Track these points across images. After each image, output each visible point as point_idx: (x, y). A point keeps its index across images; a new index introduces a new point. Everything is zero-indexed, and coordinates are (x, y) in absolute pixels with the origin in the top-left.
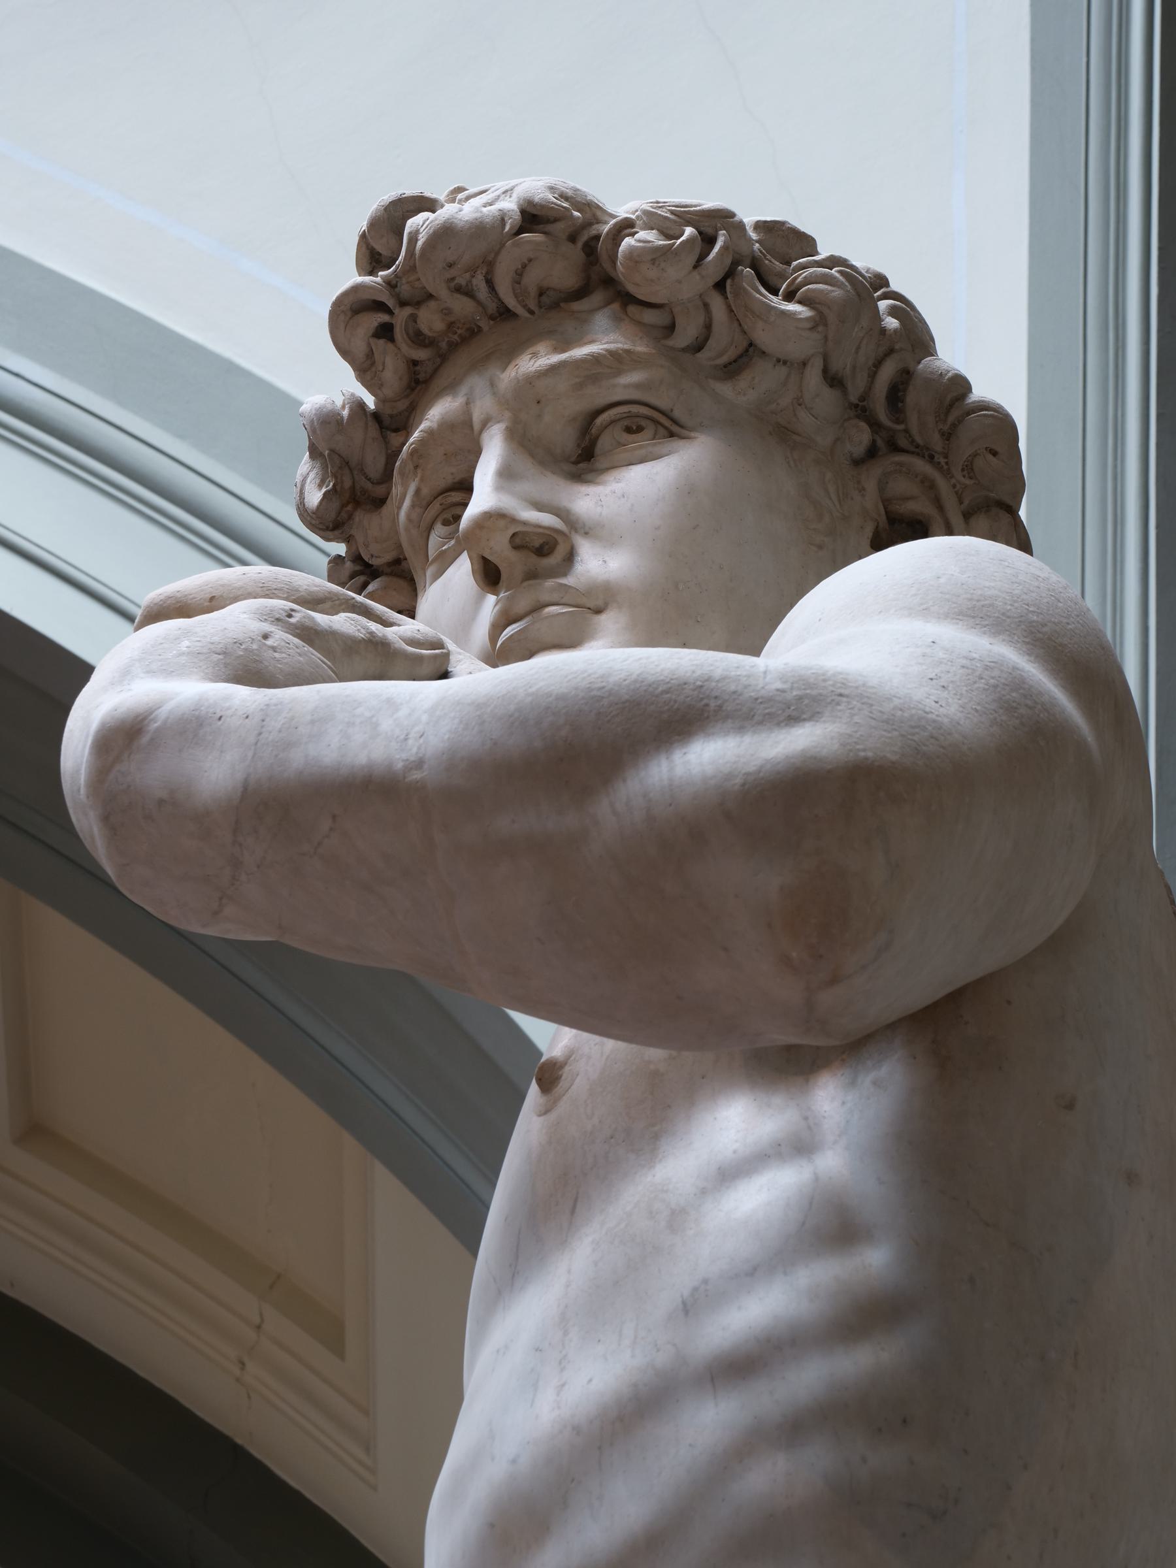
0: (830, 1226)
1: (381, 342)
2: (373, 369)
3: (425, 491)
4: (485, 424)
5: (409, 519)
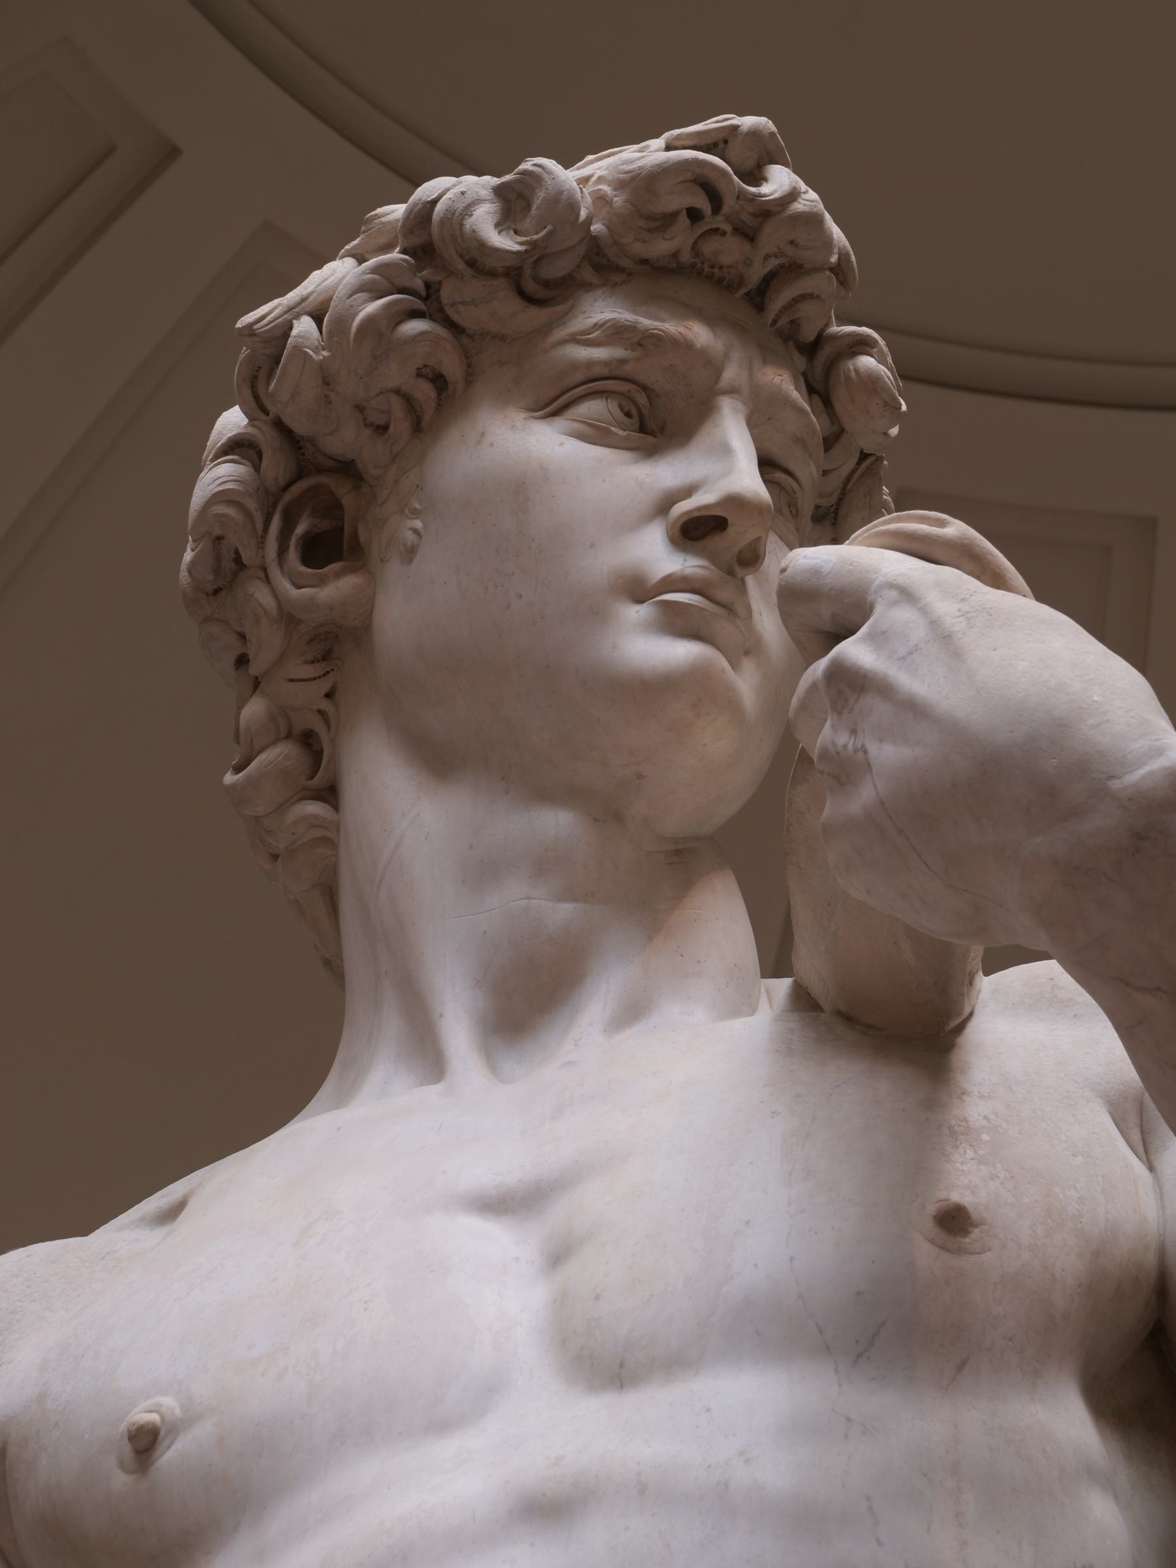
1: (688, 222)
2: (652, 224)
3: (628, 369)
4: (732, 391)
5: (590, 364)
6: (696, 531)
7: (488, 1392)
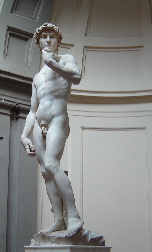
0: (65, 84)
6: (47, 42)
7: (42, 83)
